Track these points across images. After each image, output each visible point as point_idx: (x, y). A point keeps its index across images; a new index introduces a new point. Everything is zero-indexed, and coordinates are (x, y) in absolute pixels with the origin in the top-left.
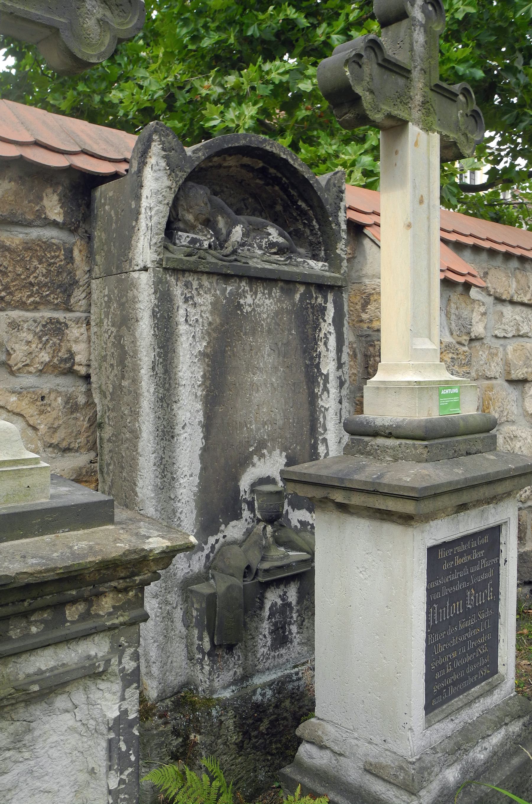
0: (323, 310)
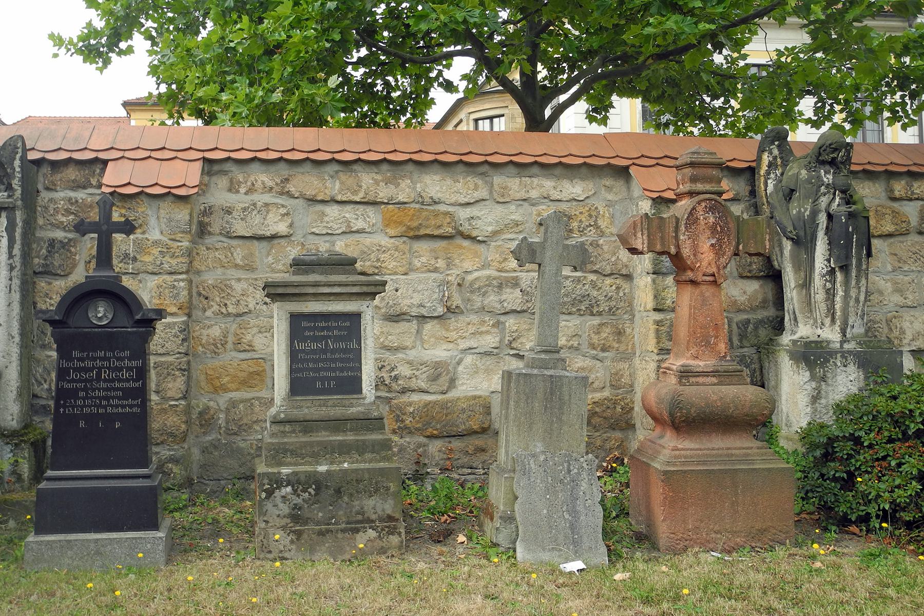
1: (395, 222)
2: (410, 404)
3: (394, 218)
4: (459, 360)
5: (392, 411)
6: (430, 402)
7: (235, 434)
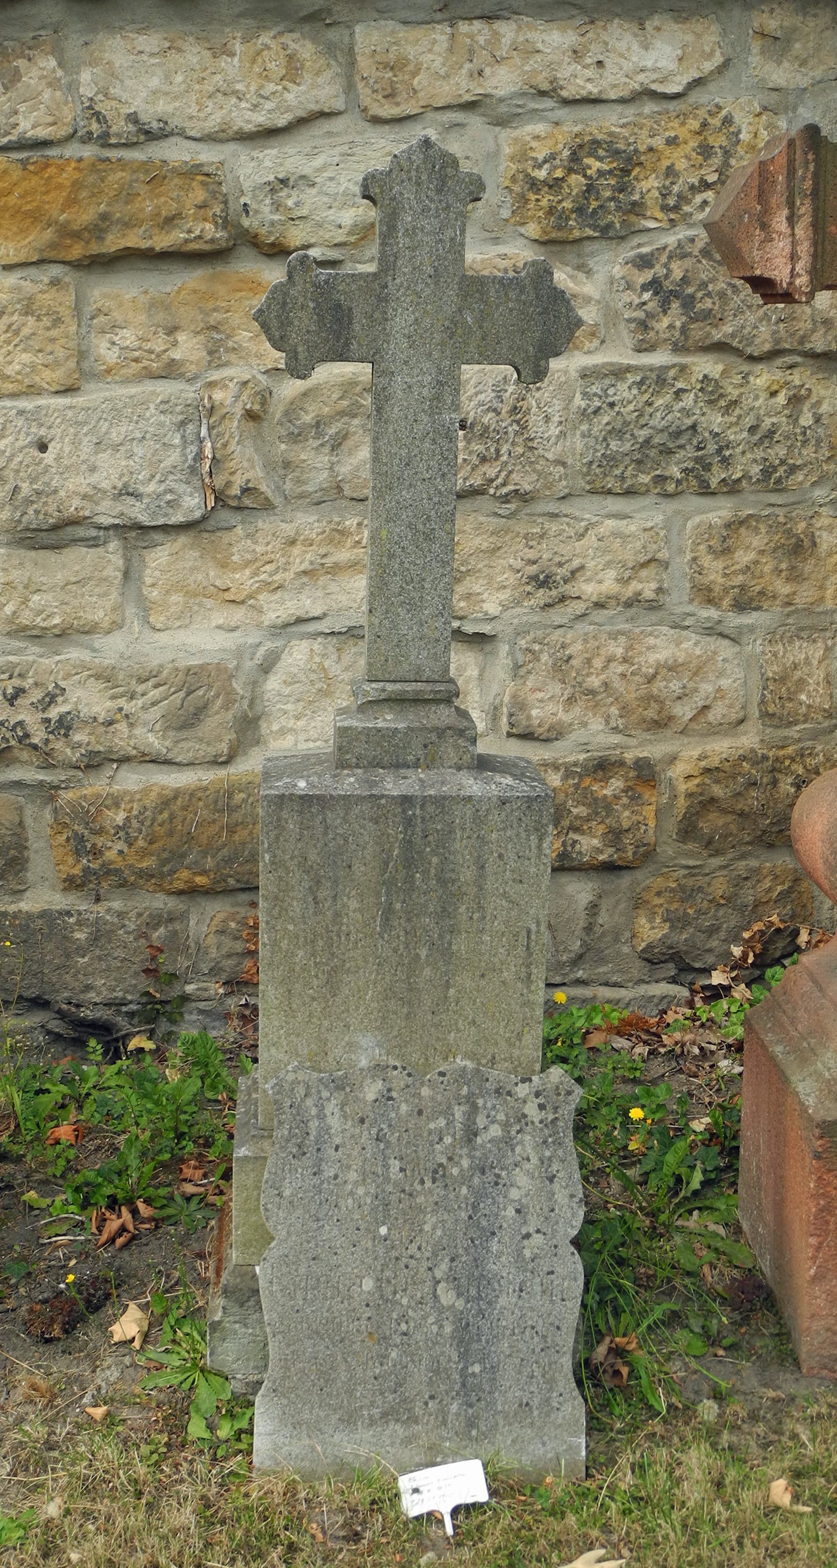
1: (16, 212)
2: (116, 803)
3: (12, 200)
4: (265, 658)
5: (60, 826)
6: (177, 793)
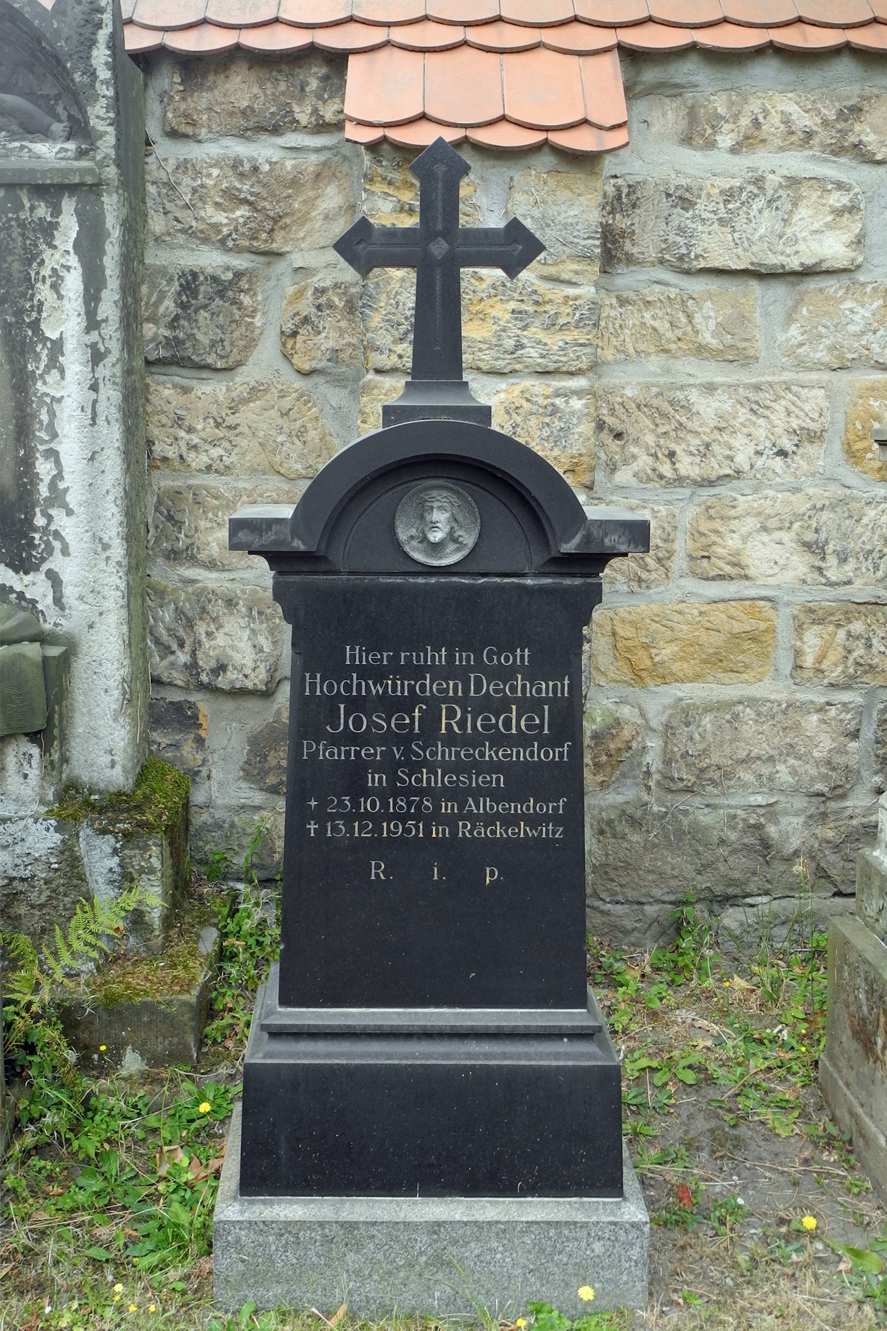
0: (49, 230)
7: (689, 790)
